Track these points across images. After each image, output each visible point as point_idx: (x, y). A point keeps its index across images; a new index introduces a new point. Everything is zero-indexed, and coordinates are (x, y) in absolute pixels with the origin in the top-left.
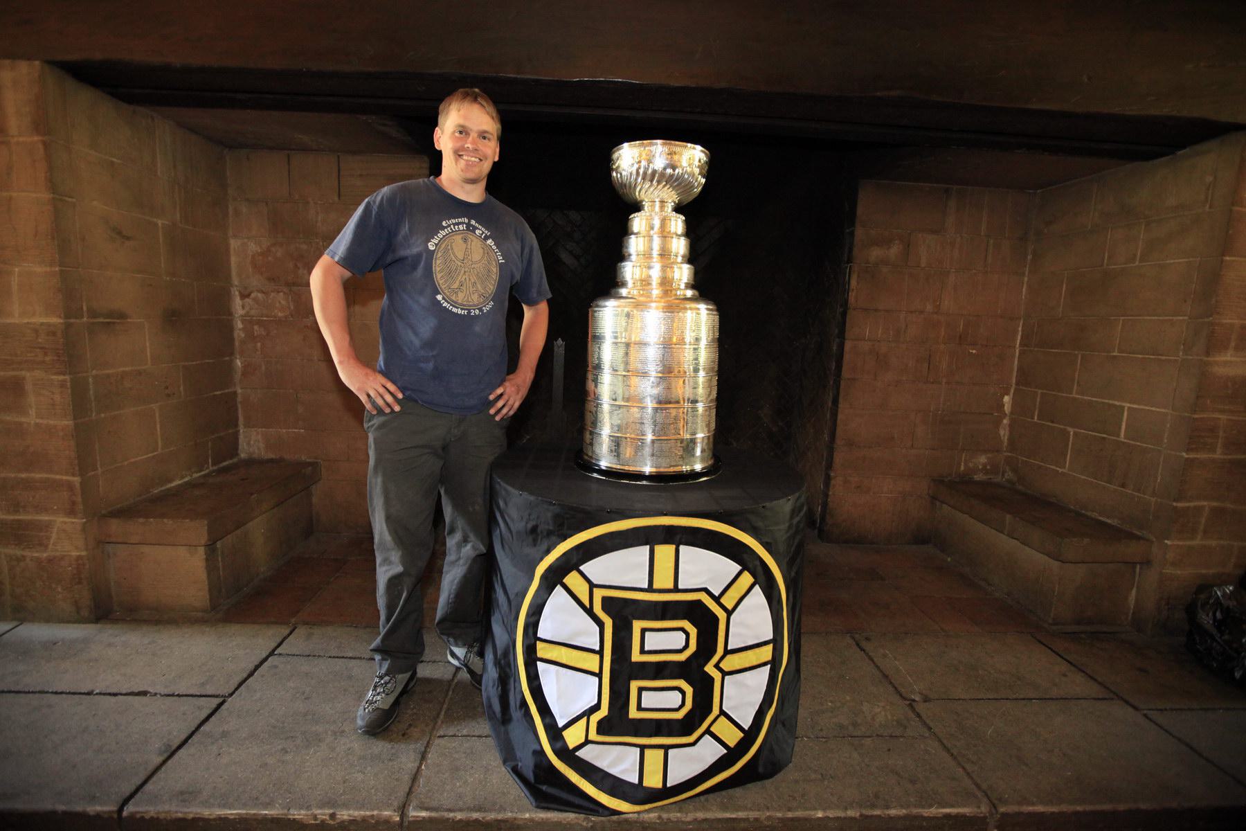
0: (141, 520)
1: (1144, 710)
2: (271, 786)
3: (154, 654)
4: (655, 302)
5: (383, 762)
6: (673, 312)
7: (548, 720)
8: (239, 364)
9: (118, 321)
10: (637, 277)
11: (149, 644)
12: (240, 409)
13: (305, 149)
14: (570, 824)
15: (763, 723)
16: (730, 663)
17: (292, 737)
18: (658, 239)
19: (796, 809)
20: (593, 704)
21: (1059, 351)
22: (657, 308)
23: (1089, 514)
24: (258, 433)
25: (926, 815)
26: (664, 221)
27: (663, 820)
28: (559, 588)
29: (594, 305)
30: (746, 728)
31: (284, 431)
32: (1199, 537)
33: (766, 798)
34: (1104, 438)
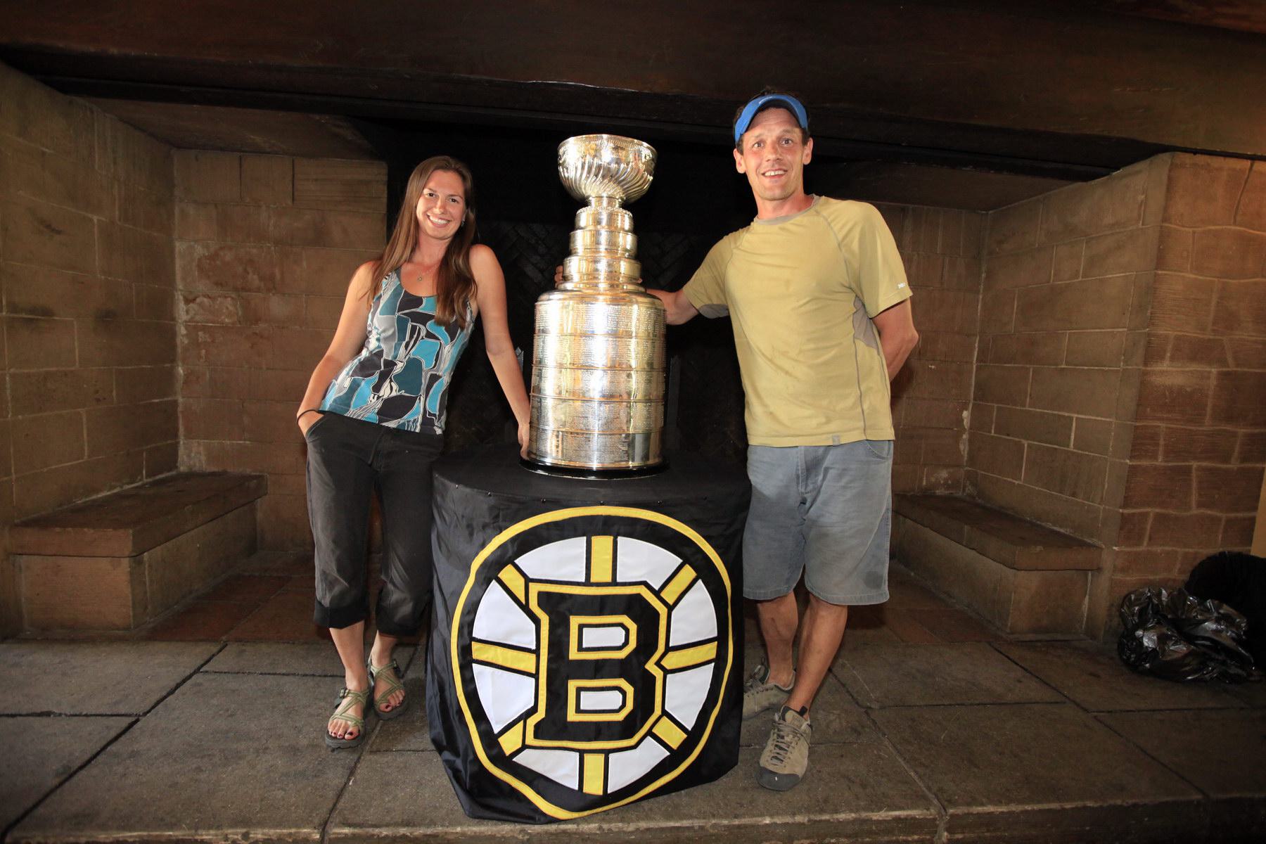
0: (58, 529)
1: (1094, 712)
2: (179, 806)
3: (64, 674)
4: (599, 294)
5: (308, 779)
6: (615, 305)
7: (483, 727)
8: (181, 372)
9: (43, 318)
10: (584, 271)
11: (60, 663)
12: (181, 421)
13: (260, 152)
14: (503, 837)
15: (707, 725)
16: (671, 661)
17: (209, 755)
18: (606, 233)
19: (743, 816)
20: (529, 707)
21: (1012, 365)
22: (605, 300)
23: (1043, 524)
24: (199, 444)
25: (875, 818)
26: (611, 217)
27: (604, 830)
28: (494, 581)
29: (539, 299)
30: (690, 729)
31: (228, 442)
32: (1145, 543)
33: (711, 806)
34: (1056, 449)
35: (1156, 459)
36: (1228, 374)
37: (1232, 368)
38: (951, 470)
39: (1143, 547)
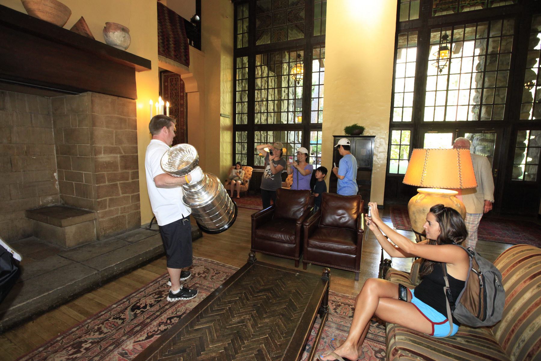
32: (108, 207)
37: (124, 154)
38: (54, 196)
39: (107, 209)
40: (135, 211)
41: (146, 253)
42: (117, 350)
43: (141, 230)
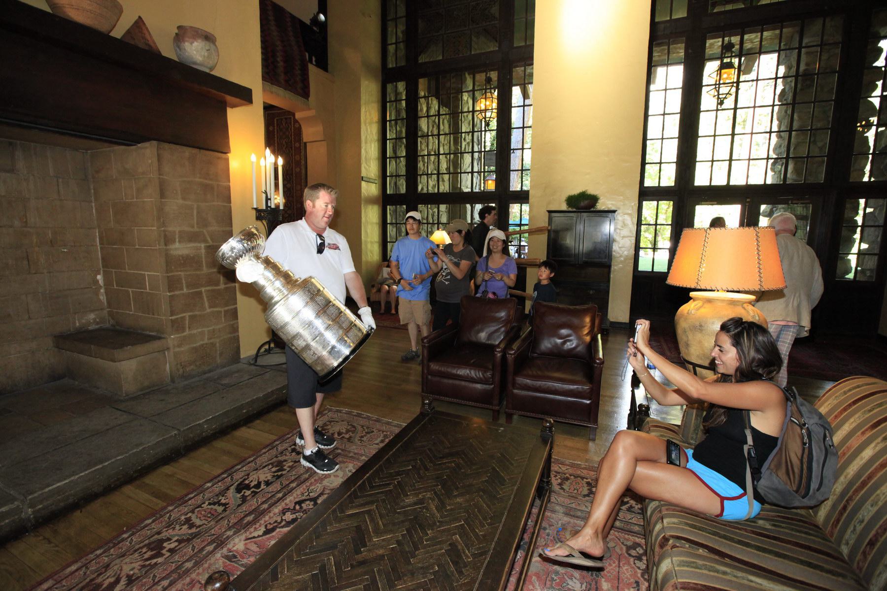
35: (183, 290)
36: (209, 247)
37: (211, 243)
38: (97, 312)
39: (187, 333)
40: (229, 336)
41: (253, 401)
42: (220, 552)
43: (239, 366)
